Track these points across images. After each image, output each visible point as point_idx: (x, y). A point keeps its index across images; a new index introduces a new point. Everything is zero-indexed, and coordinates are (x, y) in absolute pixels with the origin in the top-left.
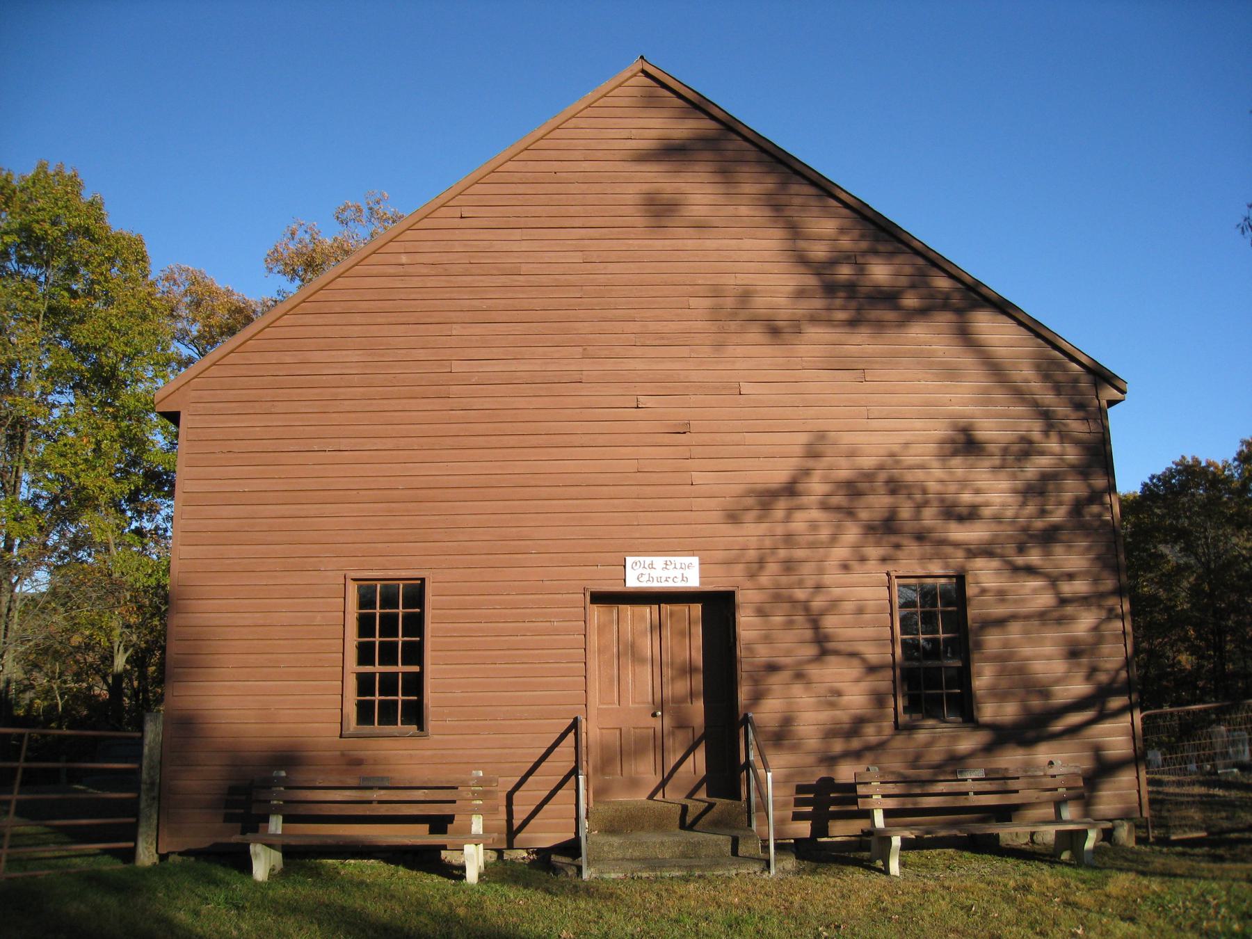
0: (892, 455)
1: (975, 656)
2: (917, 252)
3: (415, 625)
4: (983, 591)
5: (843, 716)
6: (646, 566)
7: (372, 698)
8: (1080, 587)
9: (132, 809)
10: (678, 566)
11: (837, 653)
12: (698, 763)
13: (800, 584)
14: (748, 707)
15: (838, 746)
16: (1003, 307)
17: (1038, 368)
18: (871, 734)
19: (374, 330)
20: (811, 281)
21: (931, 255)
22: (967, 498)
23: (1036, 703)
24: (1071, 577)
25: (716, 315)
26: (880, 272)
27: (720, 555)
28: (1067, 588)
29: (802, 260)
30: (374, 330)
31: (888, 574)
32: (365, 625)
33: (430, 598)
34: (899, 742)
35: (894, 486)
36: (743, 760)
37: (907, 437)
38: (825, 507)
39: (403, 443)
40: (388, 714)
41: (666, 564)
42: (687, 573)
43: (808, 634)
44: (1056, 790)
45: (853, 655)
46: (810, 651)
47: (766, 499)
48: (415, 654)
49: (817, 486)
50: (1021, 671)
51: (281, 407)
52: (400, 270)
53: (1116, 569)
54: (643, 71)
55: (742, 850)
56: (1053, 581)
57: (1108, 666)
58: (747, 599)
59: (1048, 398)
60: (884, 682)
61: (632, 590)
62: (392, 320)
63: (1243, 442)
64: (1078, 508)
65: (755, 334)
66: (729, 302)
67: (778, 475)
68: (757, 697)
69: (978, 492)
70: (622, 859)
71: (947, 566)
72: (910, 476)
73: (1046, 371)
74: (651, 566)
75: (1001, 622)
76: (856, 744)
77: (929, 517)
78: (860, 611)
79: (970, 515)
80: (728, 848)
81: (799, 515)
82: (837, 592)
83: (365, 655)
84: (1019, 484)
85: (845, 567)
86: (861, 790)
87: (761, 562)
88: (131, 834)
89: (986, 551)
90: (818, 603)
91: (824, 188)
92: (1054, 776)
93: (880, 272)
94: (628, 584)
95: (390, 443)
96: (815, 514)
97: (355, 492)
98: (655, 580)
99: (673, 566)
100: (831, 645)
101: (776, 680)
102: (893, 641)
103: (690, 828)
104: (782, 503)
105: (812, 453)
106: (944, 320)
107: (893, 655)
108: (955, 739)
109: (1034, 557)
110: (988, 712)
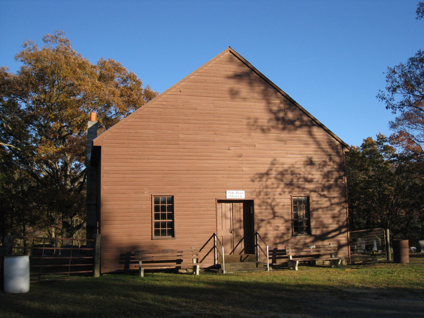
0: (292, 165)
1: (311, 218)
2: (300, 109)
3: (171, 208)
4: (313, 201)
5: (279, 233)
7: (159, 229)
8: (336, 200)
9: (92, 261)
10: (240, 193)
11: (278, 216)
12: (242, 246)
13: (269, 198)
14: (257, 230)
15: (278, 241)
16: (321, 126)
17: (328, 142)
18: (286, 238)
20: (272, 116)
21: (304, 111)
22: (310, 176)
23: (325, 230)
24: (334, 198)
25: (248, 124)
26: (290, 115)
27: (250, 190)
28: (333, 201)
29: (271, 111)
31: (291, 196)
32: (157, 209)
33: (175, 201)
34: (293, 240)
35: (293, 173)
36: (255, 244)
37: (297, 159)
38: (275, 178)
40: (164, 233)
42: (242, 195)
43: (271, 211)
44: (331, 250)
45: (282, 217)
46: (271, 216)
47: (261, 176)
48: (171, 216)
49: (274, 173)
50: (321, 222)
52: (163, 106)
53: (345, 196)
54: (230, 51)
55: (259, 266)
56: (330, 199)
57: (342, 220)
58: (257, 202)
59: (330, 151)
60: (289, 224)
63: (364, 140)
64: (336, 180)
65: (258, 131)
66: (252, 121)
67: (264, 169)
68: (259, 227)
69: (313, 175)
70: (230, 269)
71: (305, 194)
72: (297, 171)
73: (331, 144)
74: (233, 193)
75: (317, 209)
76: (282, 240)
77: (301, 182)
78: (284, 206)
79: (310, 181)
80: (255, 266)
81: (269, 180)
82: (278, 200)
83: (157, 217)
84: (323, 173)
85: (280, 194)
86: (287, 251)
87: (260, 192)
88: (92, 268)
89: (314, 191)
90: (273, 204)
91: (277, 90)
92: (330, 247)
93: (290, 115)
94: (227, 198)
95: (163, 157)
96: (273, 180)
97: (153, 171)
100: (277, 214)
101: (263, 224)
102: (292, 213)
103: (243, 261)
104: (265, 176)
105: (273, 164)
106: (305, 129)
107: (292, 217)
108: (306, 239)
109: (325, 193)
110: (314, 232)
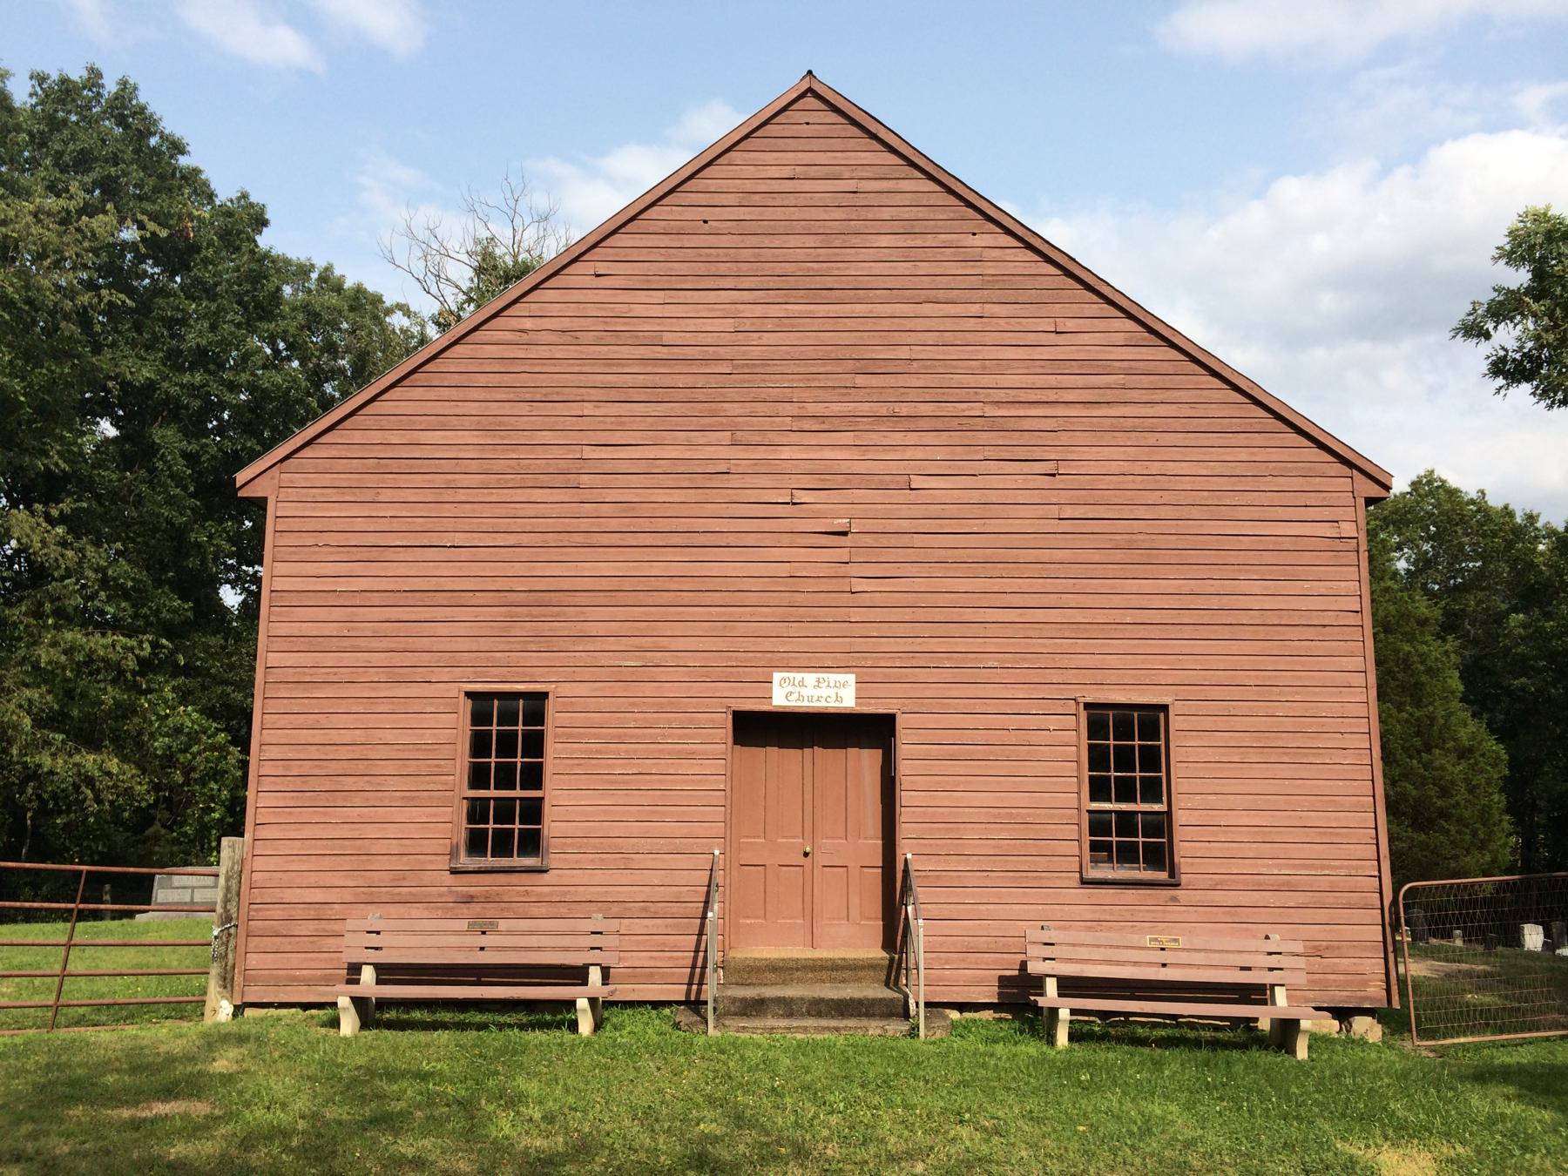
3: (535, 745)
6: (796, 683)
10: (832, 684)
19: (494, 408)
30: (494, 408)
39: (525, 539)
41: (819, 682)
42: (842, 692)
48: (534, 777)
51: (386, 495)
61: (781, 710)
62: (511, 397)
74: (802, 684)
83: (478, 777)
98: (806, 698)
99: (826, 684)
